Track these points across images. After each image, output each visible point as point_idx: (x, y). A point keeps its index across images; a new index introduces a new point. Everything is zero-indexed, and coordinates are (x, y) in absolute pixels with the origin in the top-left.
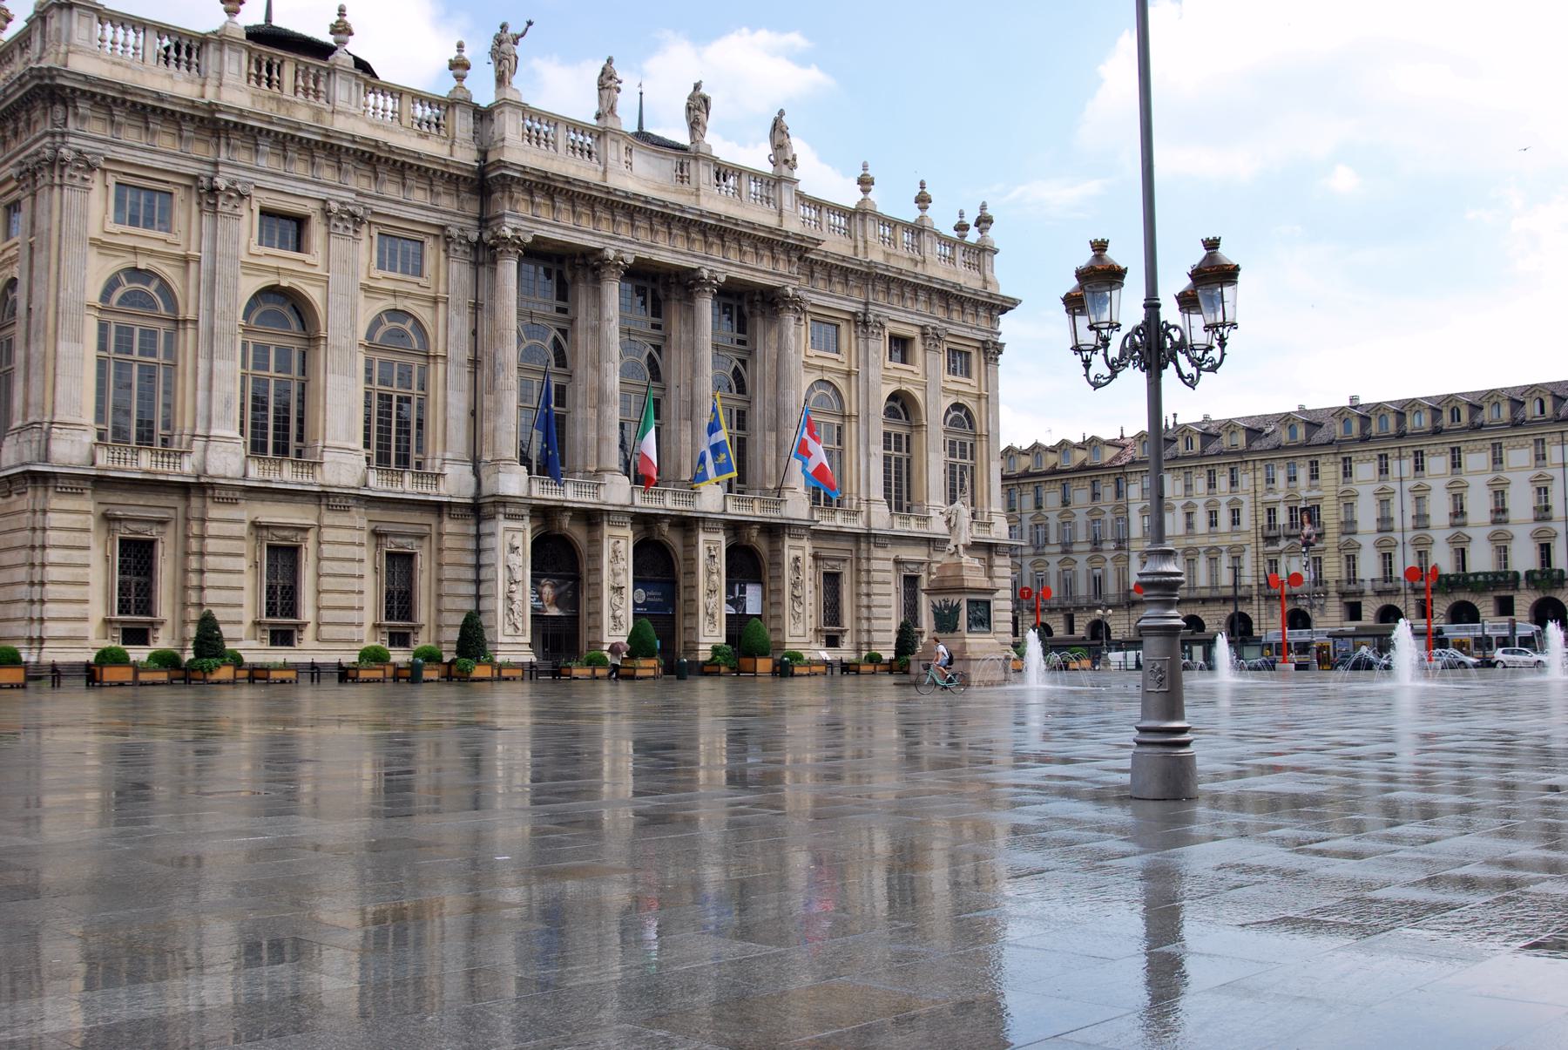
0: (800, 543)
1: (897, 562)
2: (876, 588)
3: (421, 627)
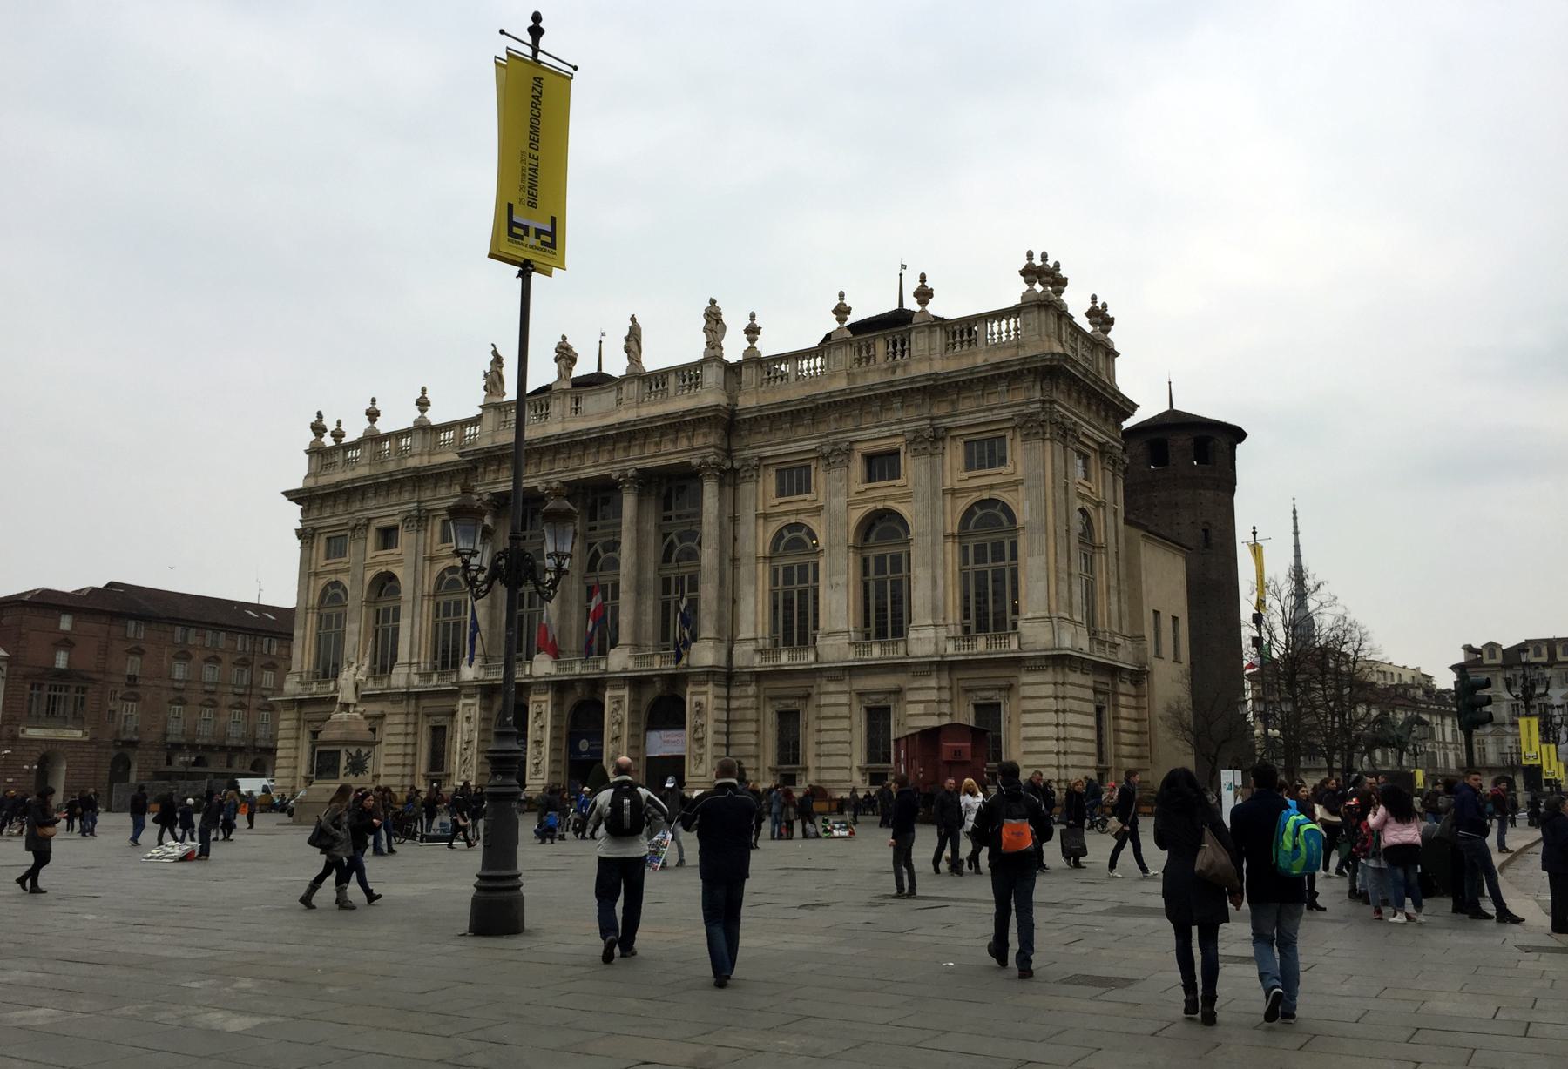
0: (704, 689)
1: (860, 694)
2: (825, 725)
3: (449, 775)
